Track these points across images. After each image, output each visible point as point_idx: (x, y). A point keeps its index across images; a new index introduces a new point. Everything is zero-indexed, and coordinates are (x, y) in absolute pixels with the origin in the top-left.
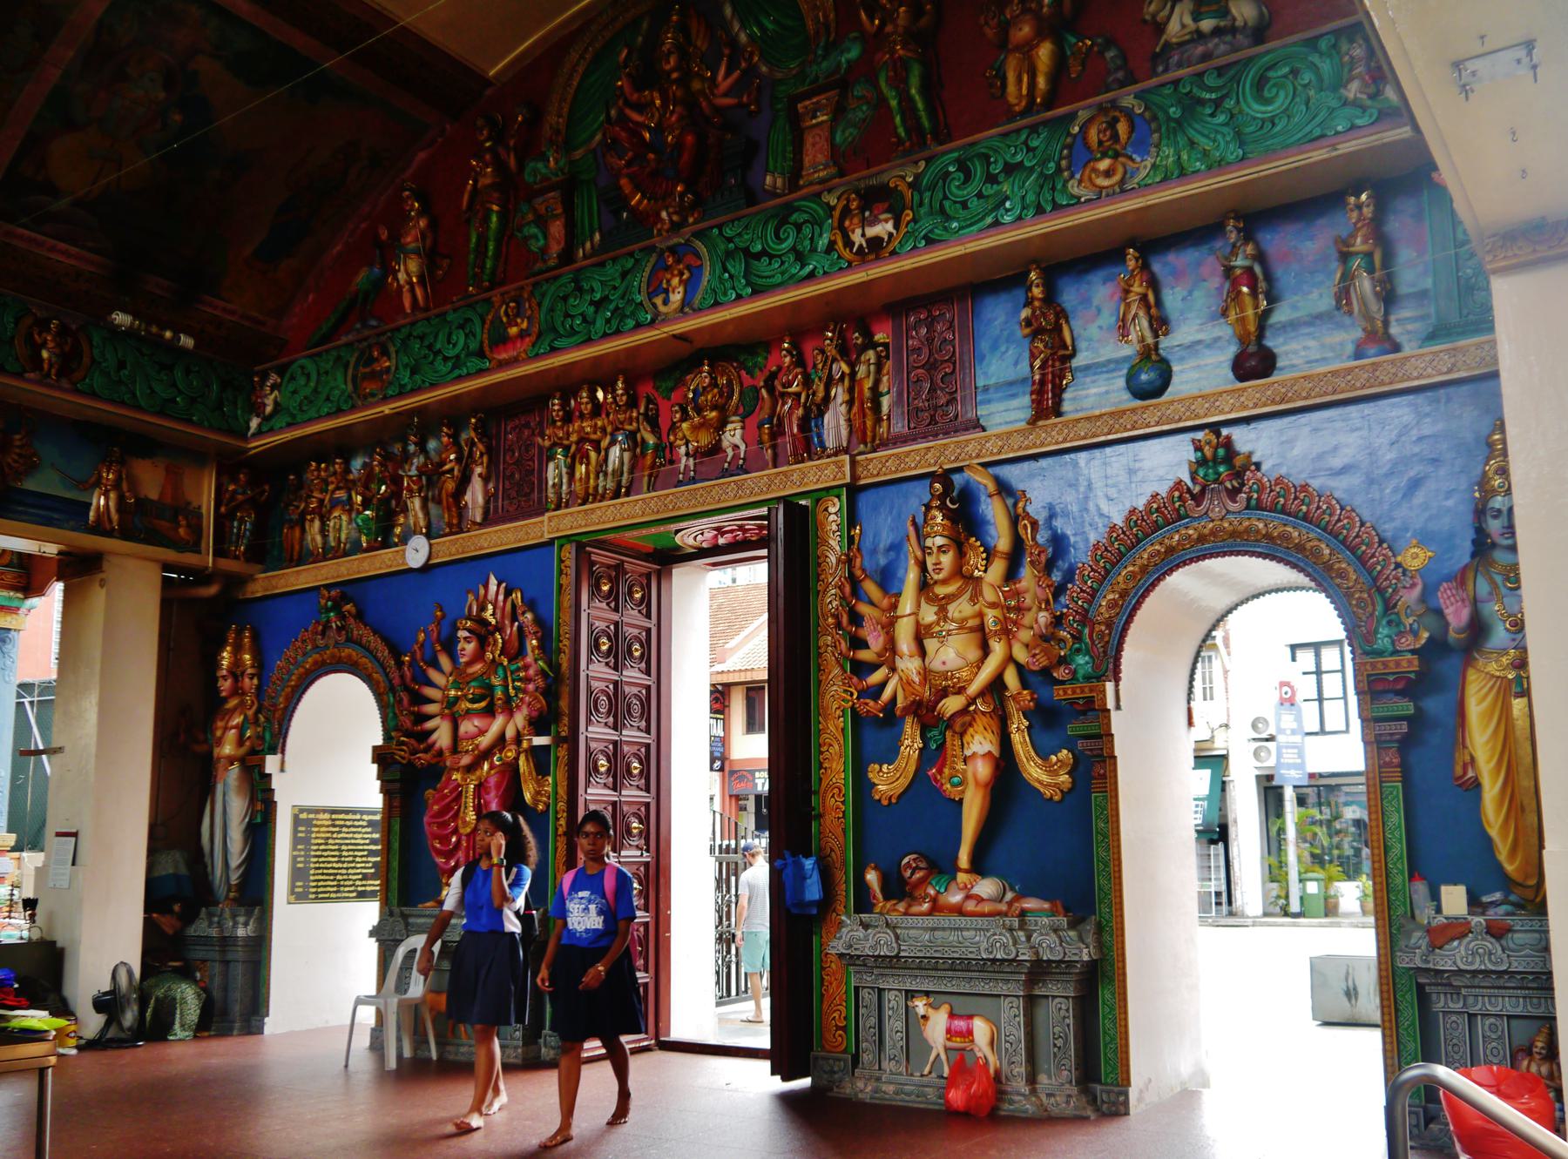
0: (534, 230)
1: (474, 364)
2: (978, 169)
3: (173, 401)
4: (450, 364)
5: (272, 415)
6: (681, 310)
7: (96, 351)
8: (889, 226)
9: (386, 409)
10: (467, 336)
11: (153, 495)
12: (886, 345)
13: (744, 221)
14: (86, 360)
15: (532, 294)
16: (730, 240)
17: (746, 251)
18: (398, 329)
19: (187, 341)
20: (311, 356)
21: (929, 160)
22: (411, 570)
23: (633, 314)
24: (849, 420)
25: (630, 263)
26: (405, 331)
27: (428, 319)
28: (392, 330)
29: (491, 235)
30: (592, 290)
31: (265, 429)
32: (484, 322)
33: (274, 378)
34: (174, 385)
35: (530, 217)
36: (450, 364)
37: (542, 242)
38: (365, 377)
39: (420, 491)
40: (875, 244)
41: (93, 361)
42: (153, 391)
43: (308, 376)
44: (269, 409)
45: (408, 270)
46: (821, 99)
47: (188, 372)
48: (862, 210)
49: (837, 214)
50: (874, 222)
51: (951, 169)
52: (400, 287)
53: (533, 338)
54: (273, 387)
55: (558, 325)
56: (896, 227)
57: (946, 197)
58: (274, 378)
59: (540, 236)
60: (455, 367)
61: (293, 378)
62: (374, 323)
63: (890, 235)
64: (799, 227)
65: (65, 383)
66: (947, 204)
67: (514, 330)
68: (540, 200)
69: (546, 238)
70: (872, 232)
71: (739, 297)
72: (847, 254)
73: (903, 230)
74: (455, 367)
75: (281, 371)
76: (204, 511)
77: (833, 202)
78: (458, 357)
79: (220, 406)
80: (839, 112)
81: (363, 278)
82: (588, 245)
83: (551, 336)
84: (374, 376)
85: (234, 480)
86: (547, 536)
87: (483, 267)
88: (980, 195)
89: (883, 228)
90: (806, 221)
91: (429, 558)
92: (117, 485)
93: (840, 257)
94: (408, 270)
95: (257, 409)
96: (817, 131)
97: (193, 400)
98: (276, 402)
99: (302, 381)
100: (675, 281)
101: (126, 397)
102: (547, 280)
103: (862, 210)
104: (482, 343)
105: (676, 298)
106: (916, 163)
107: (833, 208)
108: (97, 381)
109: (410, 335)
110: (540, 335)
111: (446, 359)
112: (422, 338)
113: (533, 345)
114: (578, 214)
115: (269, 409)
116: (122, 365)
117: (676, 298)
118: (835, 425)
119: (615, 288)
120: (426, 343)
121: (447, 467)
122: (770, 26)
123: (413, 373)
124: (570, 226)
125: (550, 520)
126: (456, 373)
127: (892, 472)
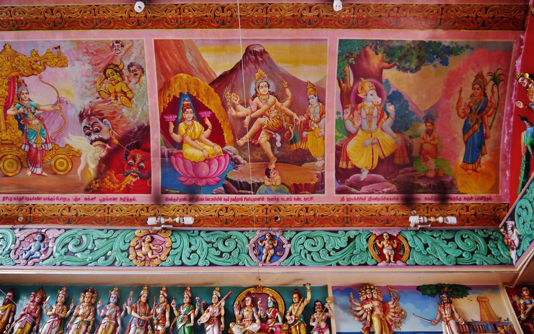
3: (461, 256)
5: (520, 245)
7: (410, 243)
11: (477, 318)
14: (407, 249)
19: (452, 220)
20: (521, 198)
31: (519, 254)
33: (510, 224)
34: (458, 248)
41: (410, 248)
42: (448, 255)
43: (526, 208)
44: (517, 242)
47: (463, 239)
54: (512, 229)
58: (510, 224)
61: (519, 216)
65: (399, 263)
75: (512, 217)
76: (511, 320)
79: (489, 252)
85: (521, 297)
92: (452, 317)
95: (509, 246)
97: (472, 253)
98: (519, 236)
99: (524, 213)
101: (435, 261)
108: (416, 258)
115: (517, 242)
116: (426, 246)
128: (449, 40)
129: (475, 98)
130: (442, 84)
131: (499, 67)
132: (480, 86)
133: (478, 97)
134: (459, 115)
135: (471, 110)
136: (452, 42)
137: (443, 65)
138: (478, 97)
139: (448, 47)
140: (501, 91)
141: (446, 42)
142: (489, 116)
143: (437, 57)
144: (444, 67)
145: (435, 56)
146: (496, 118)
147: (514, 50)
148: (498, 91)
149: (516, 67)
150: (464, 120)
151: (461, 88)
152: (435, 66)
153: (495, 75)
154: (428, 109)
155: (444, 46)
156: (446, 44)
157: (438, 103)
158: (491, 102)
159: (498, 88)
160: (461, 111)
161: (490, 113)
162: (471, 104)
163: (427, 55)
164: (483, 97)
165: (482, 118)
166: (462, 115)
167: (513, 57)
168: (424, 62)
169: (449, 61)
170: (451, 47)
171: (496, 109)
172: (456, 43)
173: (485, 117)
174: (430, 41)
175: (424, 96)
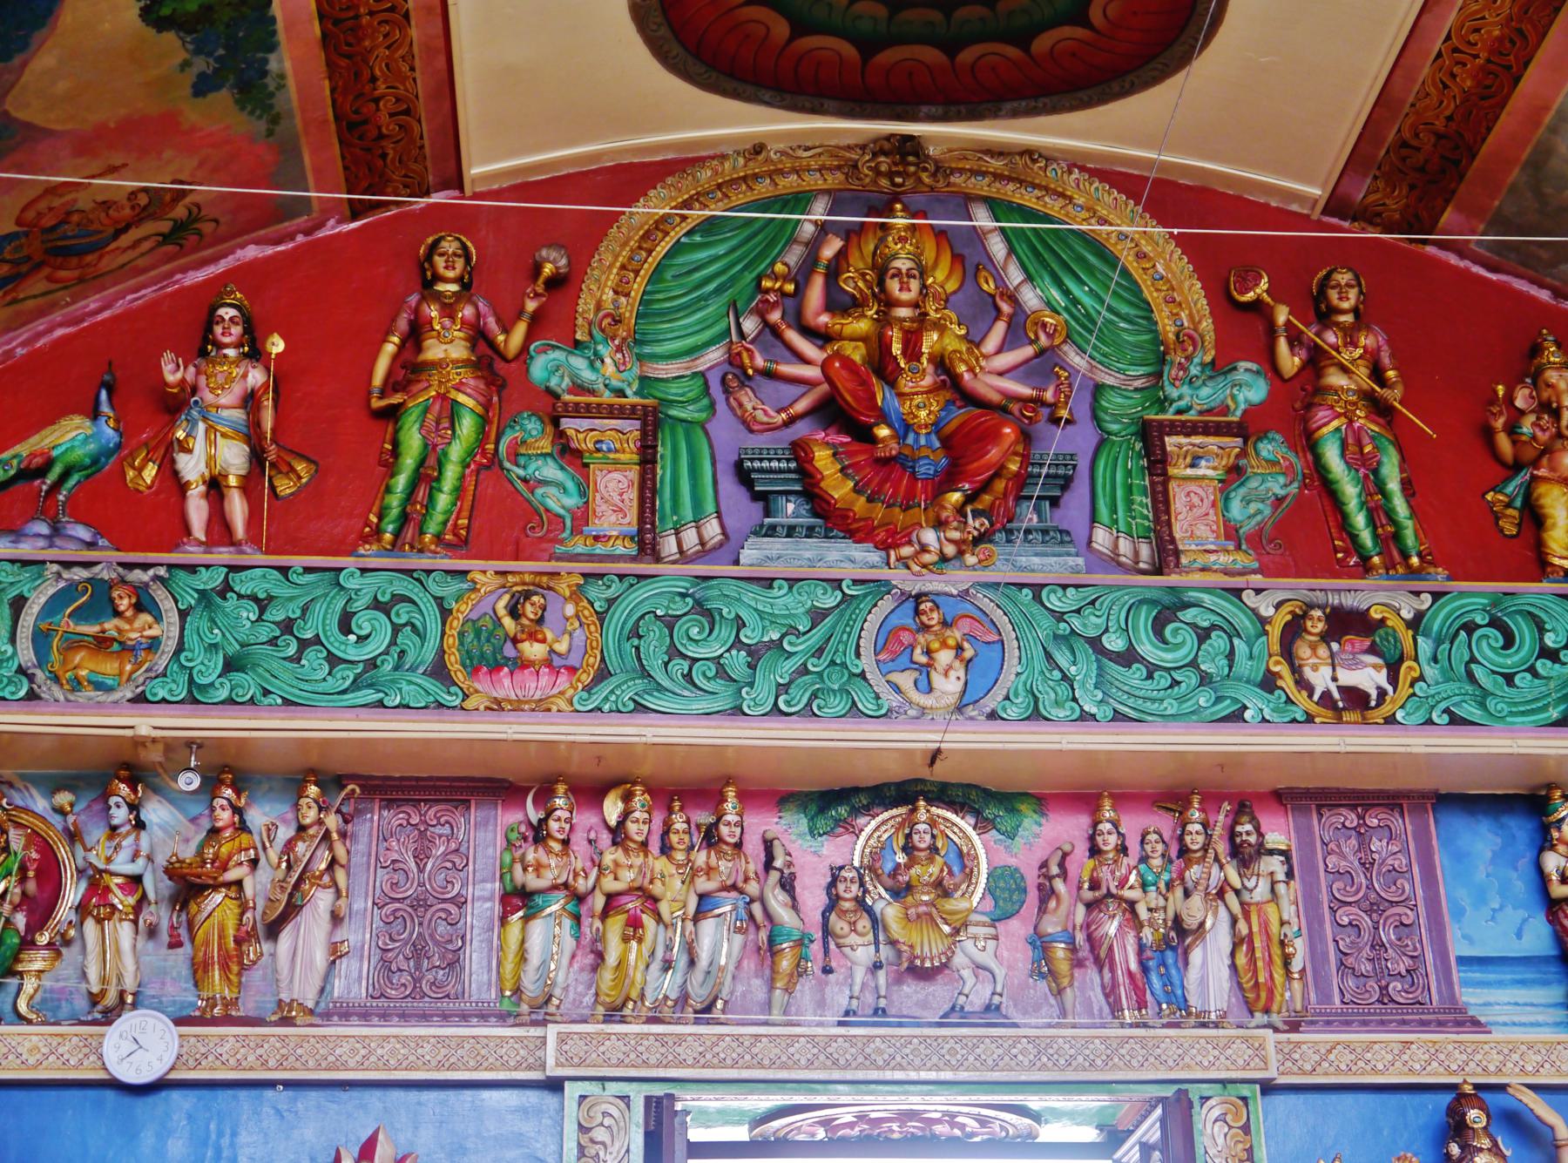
0: (550, 470)
1: (417, 687)
2: (1524, 632)
4: (347, 675)
6: (959, 709)
8: (1382, 678)
9: (145, 724)
10: (396, 629)
12: (1286, 854)
13: (1090, 594)
15: (577, 594)
16: (1060, 617)
17: (1095, 643)
18: (192, 569)
21: (1437, 596)
22: (115, 1085)
23: (844, 691)
24: (1233, 967)
25: (830, 600)
26: (210, 580)
27: (284, 570)
28: (170, 567)
29: (456, 452)
30: (740, 624)
32: (445, 613)
35: (546, 445)
36: (347, 675)
37: (573, 501)
38: (74, 644)
39: (137, 909)
40: (1356, 698)
45: (211, 451)
46: (1212, 442)
48: (1325, 638)
49: (1275, 631)
50: (1354, 665)
51: (1479, 620)
52: (174, 484)
53: (586, 679)
55: (655, 665)
56: (1393, 679)
57: (1473, 660)
59: (570, 485)
60: (356, 685)
62: (83, 533)
63: (1382, 693)
64: (1203, 635)
66: (1478, 672)
67: (534, 650)
68: (585, 424)
69: (583, 494)
70: (1348, 678)
71: (1085, 717)
72: (1301, 697)
73: (1404, 689)
74: (356, 685)
77: (1267, 611)
78: (372, 664)
80: (1235, 473)
81: (73, 438)
82: (690, 538)
83: (640, 684)
84: (102, 643)
86: (553, 1071)
87: (430, 503)
88: (1532, 670)
89: (1368, 676)
90: (1214, 627)
91: (172, 1068)
93: (1289, 701)
94: (211, 451)
96: (1193, 487)
100: (944, 657)
102: (621, 577)
103: (1325, 638)
104: (441, 652)
105: (949, 686)
106: (1417, 594)
107: (1264, 621)
109: (225, 589)
110: (603, 674)
111: (333, 660)
112: (263, 604)
113: (588, 689)
114: (663, 471)
117: (949, 686)
118: (1209, 971)
119: (792, 631)
120: (276, 614)
121: (232, 875)
122: (1087, 301)
123: (230, 666)
124: (647, 490)
125: (562, 1039)
126: (371, 696)
127: (1339, 1071)
128: (288, 65)
129: (103, 215)
130: (123, 112)
131: (222, 220)
132: (145, 208)
133: (106, 221)
134: (24, 210)
135: (53, 228)
136: (282, 76)
137: (194, 86)
138: (106, 221)
139: (265, 73)
140: (141, 262)
141: (281, 61)
142: (50, 279)
143: (218, 59)
144: (188, 91)
145: (221, 52)
146: (50, 297)
147: (287, 224)
148: (143, 254)
149: (233, 252)
150: (17, 229)
151: (125, 165)
152: (185, 65)
153: (197, 220)
154: (16, 120)
155: (266, 61)
156: (273, 65)
157: (49, 133)
158: (101, 257)
159: (152, 249)
160: (42, 206)
161: (63, 274)
162: (75, 218)
163: (222, 28)
164: (111, 230)
165: (38, 267)
166: (31, 215)
167: (262, 232)
168: (189, 32)
169: (211, 96)
170: (268, 80)
171: (81, 280)
172: (281, 87)
173: (46, 271)
174: (273, 20)
175: (62, 86)
